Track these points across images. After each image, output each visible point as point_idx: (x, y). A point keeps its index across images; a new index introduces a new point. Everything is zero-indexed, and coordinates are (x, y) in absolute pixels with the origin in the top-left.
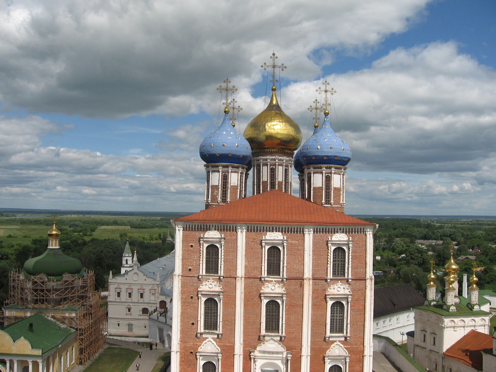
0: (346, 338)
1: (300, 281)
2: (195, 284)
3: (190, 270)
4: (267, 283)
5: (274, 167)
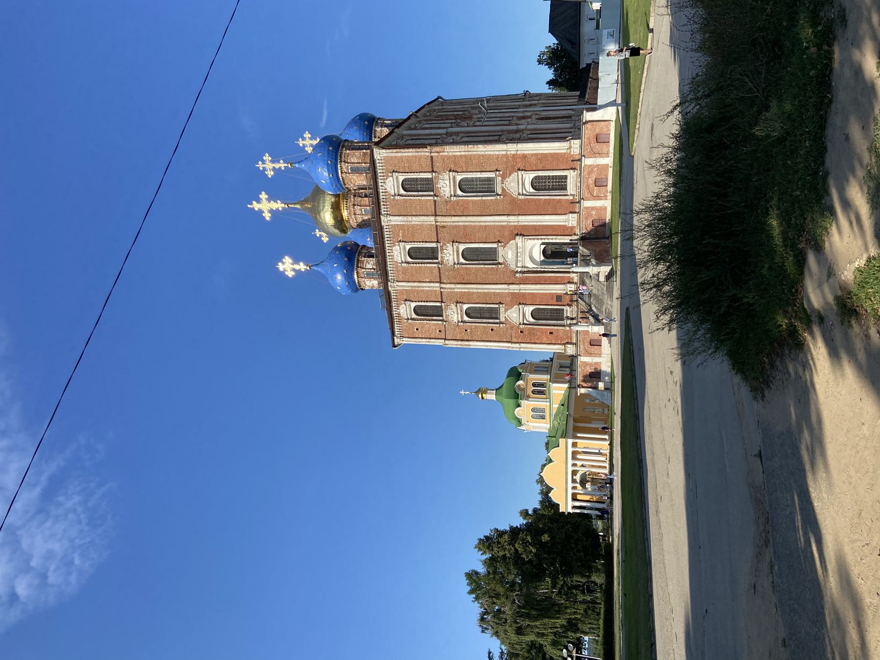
0: (499, 176)
1: (440, 230)
2: (452, 327)
3: (440, 331)
4: (445, 261)
5: (363, 210)
